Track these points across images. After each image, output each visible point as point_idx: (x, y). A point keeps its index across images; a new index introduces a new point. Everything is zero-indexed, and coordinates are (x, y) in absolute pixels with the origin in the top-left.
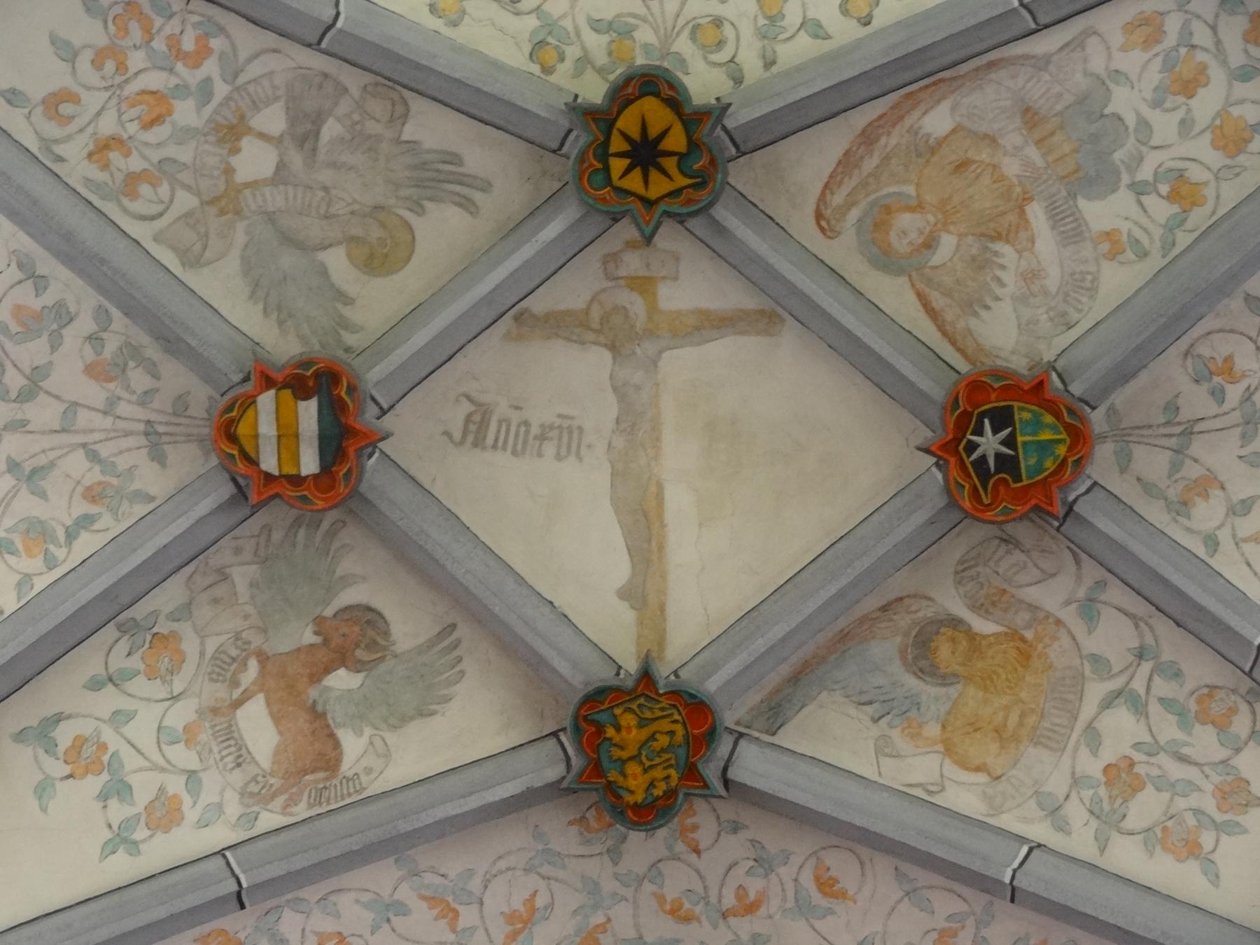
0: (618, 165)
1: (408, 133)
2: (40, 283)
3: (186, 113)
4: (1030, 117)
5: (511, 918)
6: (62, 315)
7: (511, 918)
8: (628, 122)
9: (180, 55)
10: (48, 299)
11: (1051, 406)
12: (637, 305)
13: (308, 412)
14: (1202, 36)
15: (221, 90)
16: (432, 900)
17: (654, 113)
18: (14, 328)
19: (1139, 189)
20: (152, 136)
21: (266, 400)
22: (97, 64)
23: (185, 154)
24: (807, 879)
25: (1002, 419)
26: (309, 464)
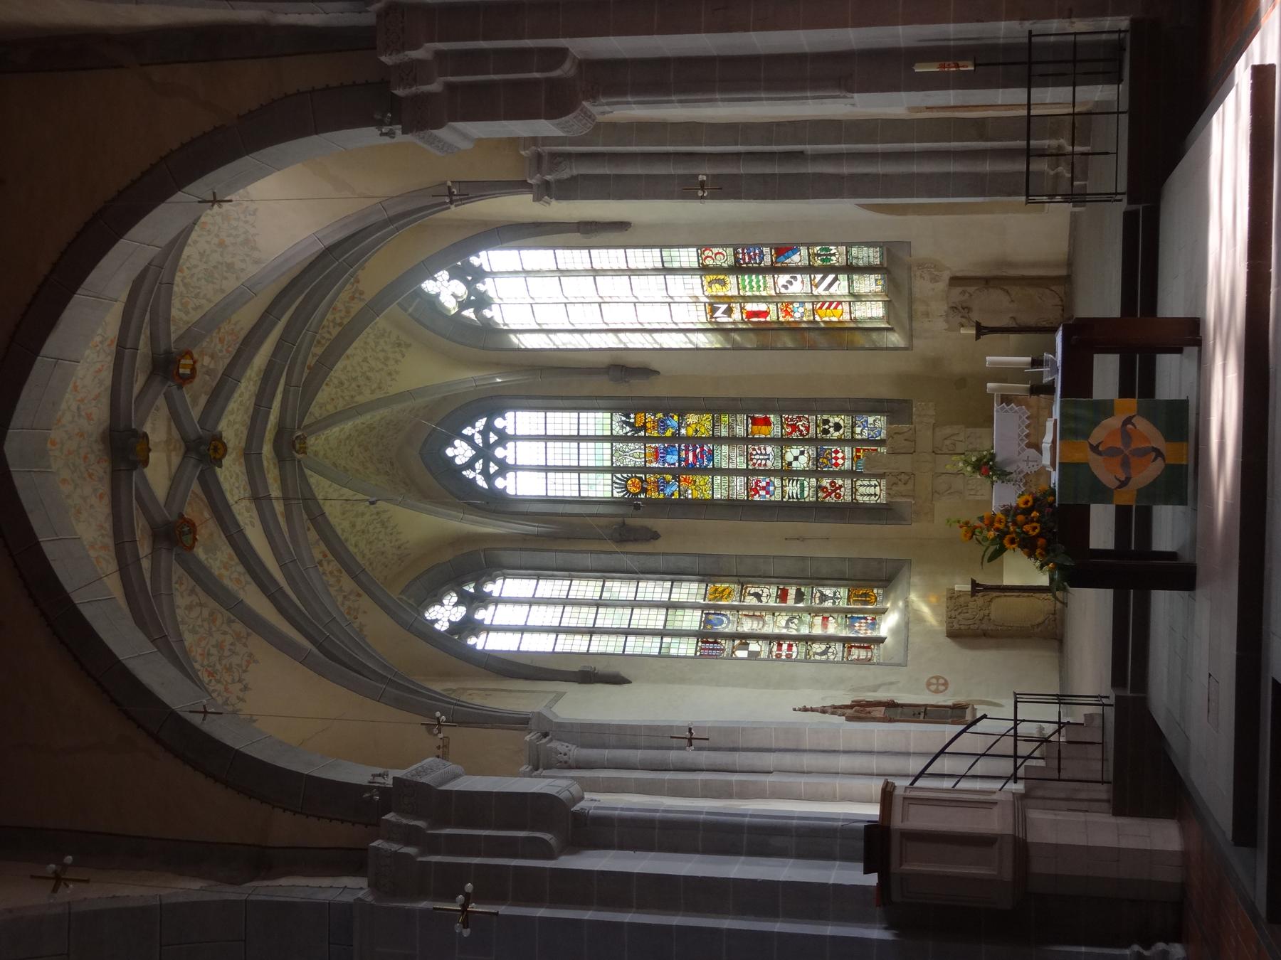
0: (213, 442)
1: (203, 395)
2: (196, 309)
3: (219, 346)
4: (211, 535)
5: (91, 414)
6: (187, 313)
7: (91, 414)
8: (220, 446)
9: (229, 347)
10: (191, 310)
11: (194, 543)
12: (172, 447)
13: (188, 371)
14: (233, 568)
15: (220, 354)
16: (99, 394)
17: (221, 451)
18: (184, 301)
19: (207, 559)
20: (218, 340)
21: (191, 362)
22: (233, 329)
23: (213, 344)
24: (101, 491)
25: (190, 532)
26: (181, 371)
